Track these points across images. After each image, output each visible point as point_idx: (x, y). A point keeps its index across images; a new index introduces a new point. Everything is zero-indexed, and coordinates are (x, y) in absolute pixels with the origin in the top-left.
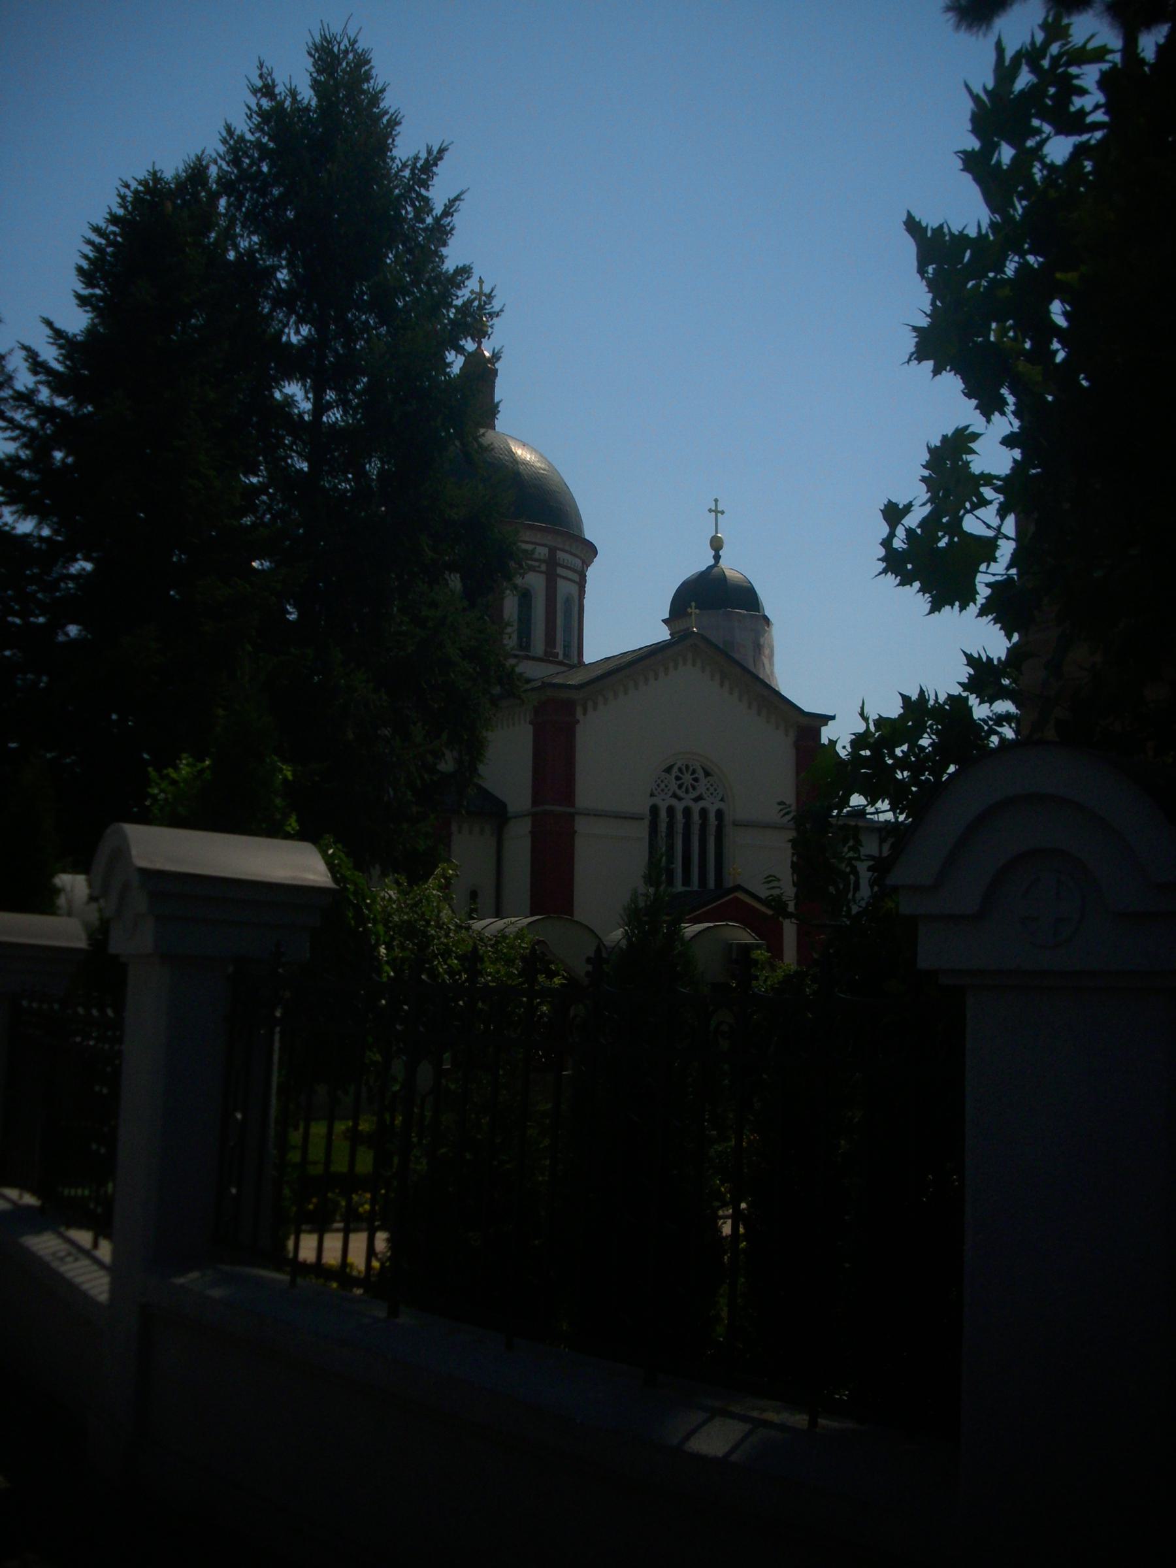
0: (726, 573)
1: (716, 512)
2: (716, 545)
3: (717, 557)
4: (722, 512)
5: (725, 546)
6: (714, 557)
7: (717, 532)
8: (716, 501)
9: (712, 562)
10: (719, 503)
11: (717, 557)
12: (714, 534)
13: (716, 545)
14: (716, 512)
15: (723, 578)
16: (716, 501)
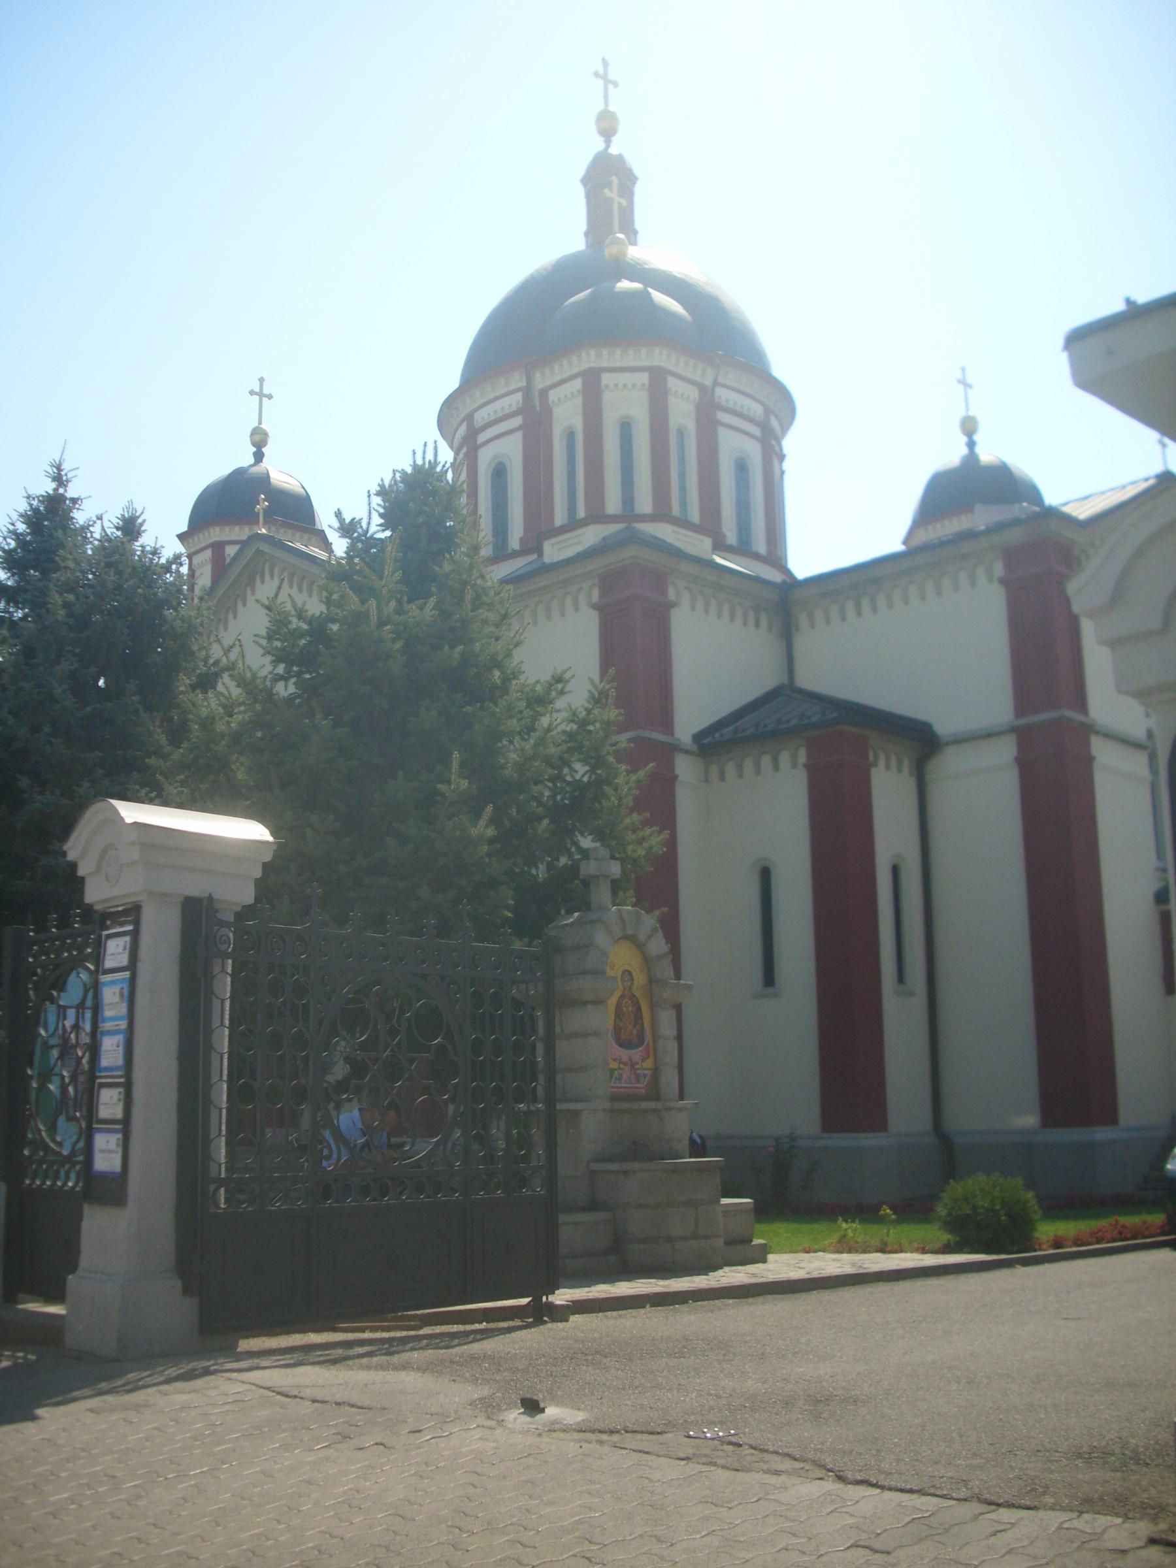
0: (271, 475)
1: (261, 395)
2: (259, 440)
3: (259, 457)
4: (270, 397)
5: (270, 441)
6: (255, 454)
7: (260, 423)
8: (261, 380)
9: (252, 461)
10: (264, 383)
11: (259, 457)
12: (256, 424)
13: (259, 440)
14: (261, 395)
15: (265, 478)
16: (261, 380)
